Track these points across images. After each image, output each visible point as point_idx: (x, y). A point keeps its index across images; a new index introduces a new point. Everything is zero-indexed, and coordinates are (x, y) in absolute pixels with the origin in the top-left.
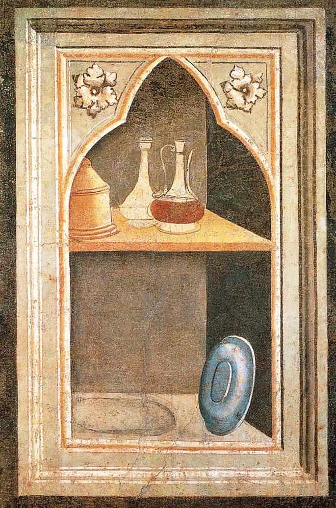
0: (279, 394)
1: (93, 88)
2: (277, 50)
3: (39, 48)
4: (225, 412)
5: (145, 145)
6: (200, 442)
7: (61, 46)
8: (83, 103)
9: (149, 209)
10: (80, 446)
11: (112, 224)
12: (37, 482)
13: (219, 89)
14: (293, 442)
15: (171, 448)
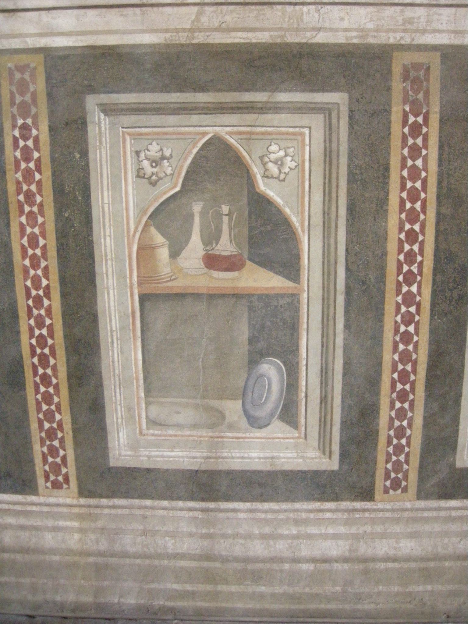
0: (304, 400)
1: (154, 161)
2: (307, 129)
3: (107, 128)
4: (261, 413)
5: (197, 208)
7: (125, 126)
8: (145, 174)
9: (201, 260)
10: (153, 435)
11: (171, 272)
12: (123, 458)
13: (258, 162)
14: (314, 432)
15: (222, 437)
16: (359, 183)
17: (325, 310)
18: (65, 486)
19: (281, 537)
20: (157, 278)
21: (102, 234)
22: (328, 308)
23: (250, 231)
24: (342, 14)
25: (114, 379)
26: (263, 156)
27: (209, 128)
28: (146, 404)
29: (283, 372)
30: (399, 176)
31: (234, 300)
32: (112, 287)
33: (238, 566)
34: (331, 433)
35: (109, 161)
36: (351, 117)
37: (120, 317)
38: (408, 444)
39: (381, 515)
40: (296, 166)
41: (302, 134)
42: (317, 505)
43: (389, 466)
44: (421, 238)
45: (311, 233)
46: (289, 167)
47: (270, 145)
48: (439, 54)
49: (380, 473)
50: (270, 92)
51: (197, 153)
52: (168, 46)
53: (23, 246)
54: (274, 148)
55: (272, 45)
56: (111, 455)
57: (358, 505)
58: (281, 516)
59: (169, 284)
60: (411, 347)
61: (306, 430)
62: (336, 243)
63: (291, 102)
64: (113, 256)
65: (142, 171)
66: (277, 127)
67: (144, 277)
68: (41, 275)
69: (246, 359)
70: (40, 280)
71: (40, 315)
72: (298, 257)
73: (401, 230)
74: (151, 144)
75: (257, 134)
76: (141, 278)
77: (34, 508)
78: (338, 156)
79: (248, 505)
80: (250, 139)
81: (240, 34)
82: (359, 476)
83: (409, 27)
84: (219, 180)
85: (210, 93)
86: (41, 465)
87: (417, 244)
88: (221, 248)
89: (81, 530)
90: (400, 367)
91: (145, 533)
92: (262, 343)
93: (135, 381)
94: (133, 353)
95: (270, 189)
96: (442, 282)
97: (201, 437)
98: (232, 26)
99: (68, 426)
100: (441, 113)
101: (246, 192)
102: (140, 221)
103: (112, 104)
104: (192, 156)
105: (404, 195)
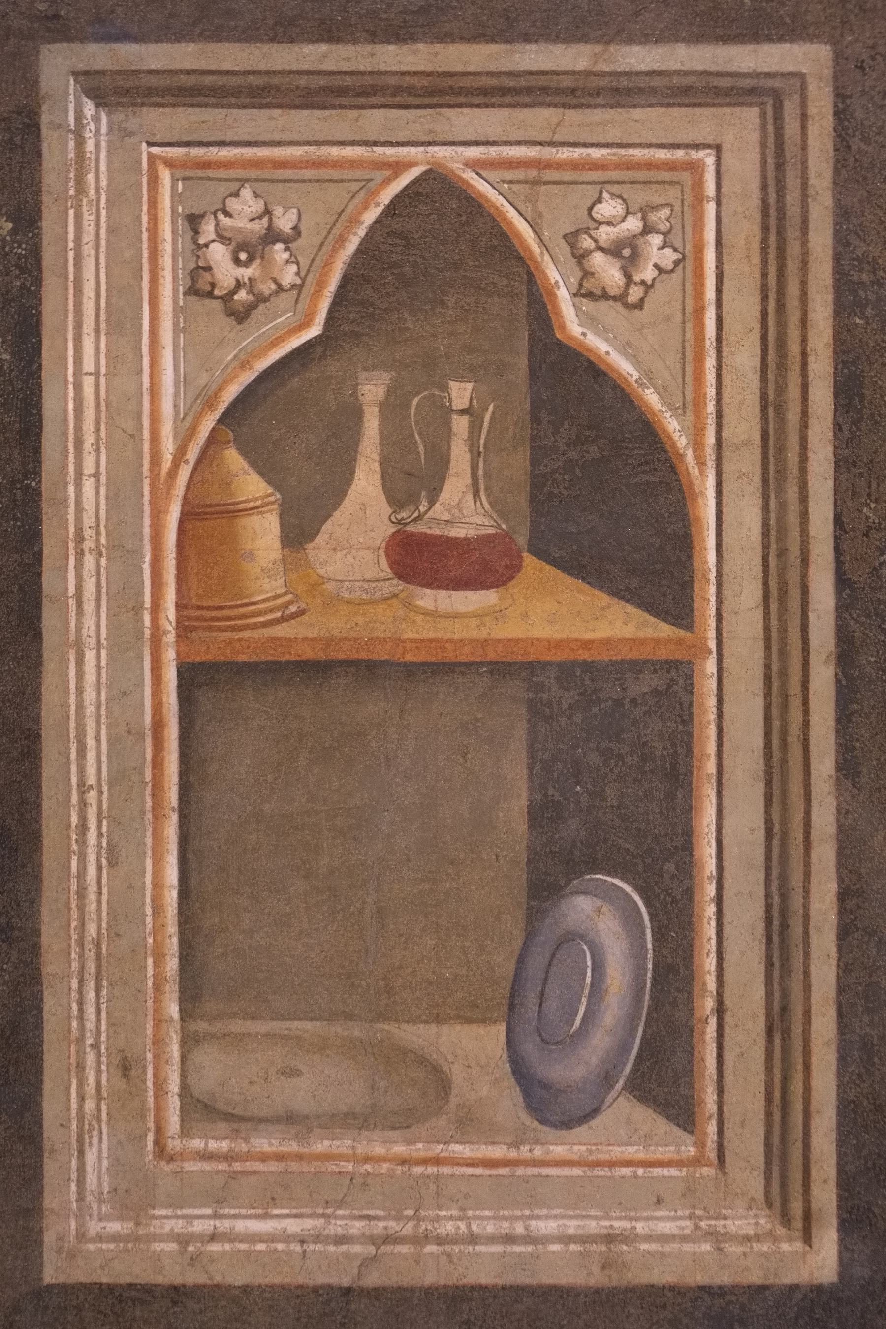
0: (713, 1022)
1: (241, 246)
2: (708, 151)
3: (103, 144)
6: (510, 1146)
7: (158, 138)
8: (213, 285)
9: (382, 552)
10: (205, 1156)
11: (286, 593)
12: (91, 1247)
15: (437, 1161)
16: (869, 312)
17: (775, 712)
20: (242, 610)
21: (71, 468)
22: (785, 707)
23: (534, 462)
25: (81, 956)
26: (576, 233)
27: (413, 150)
28: (183, 1043)
29: (641, 924)
32: (93, 641)
35: (103, 243)
36: (840, 114)
40: (677, 263)
41: (696, 168)
45: (726, 467)
46: (656, 266)
47: (599, 200)
50: (598, 41)
51: (377, 221)
54: (608, 208)
56: (49, 1238)
59: (279, 631)
61: (720, 1132)
62: (804, 499)
63: (660, 73)
64: (103, 541)
65: (207, 276)
66: (620, 145)
67: (199, 608)
74: (236, 195)
75: (559, 166)
80: (536, 182)
84: (443, 303)
85: (421, 46)
88: (446, 516)
93: (150, 961)
94: (149, 863)
95: (597, 333)
97: (367, 1159)
101: (523, 342)
103: (120, 72)
104: (362, 232)
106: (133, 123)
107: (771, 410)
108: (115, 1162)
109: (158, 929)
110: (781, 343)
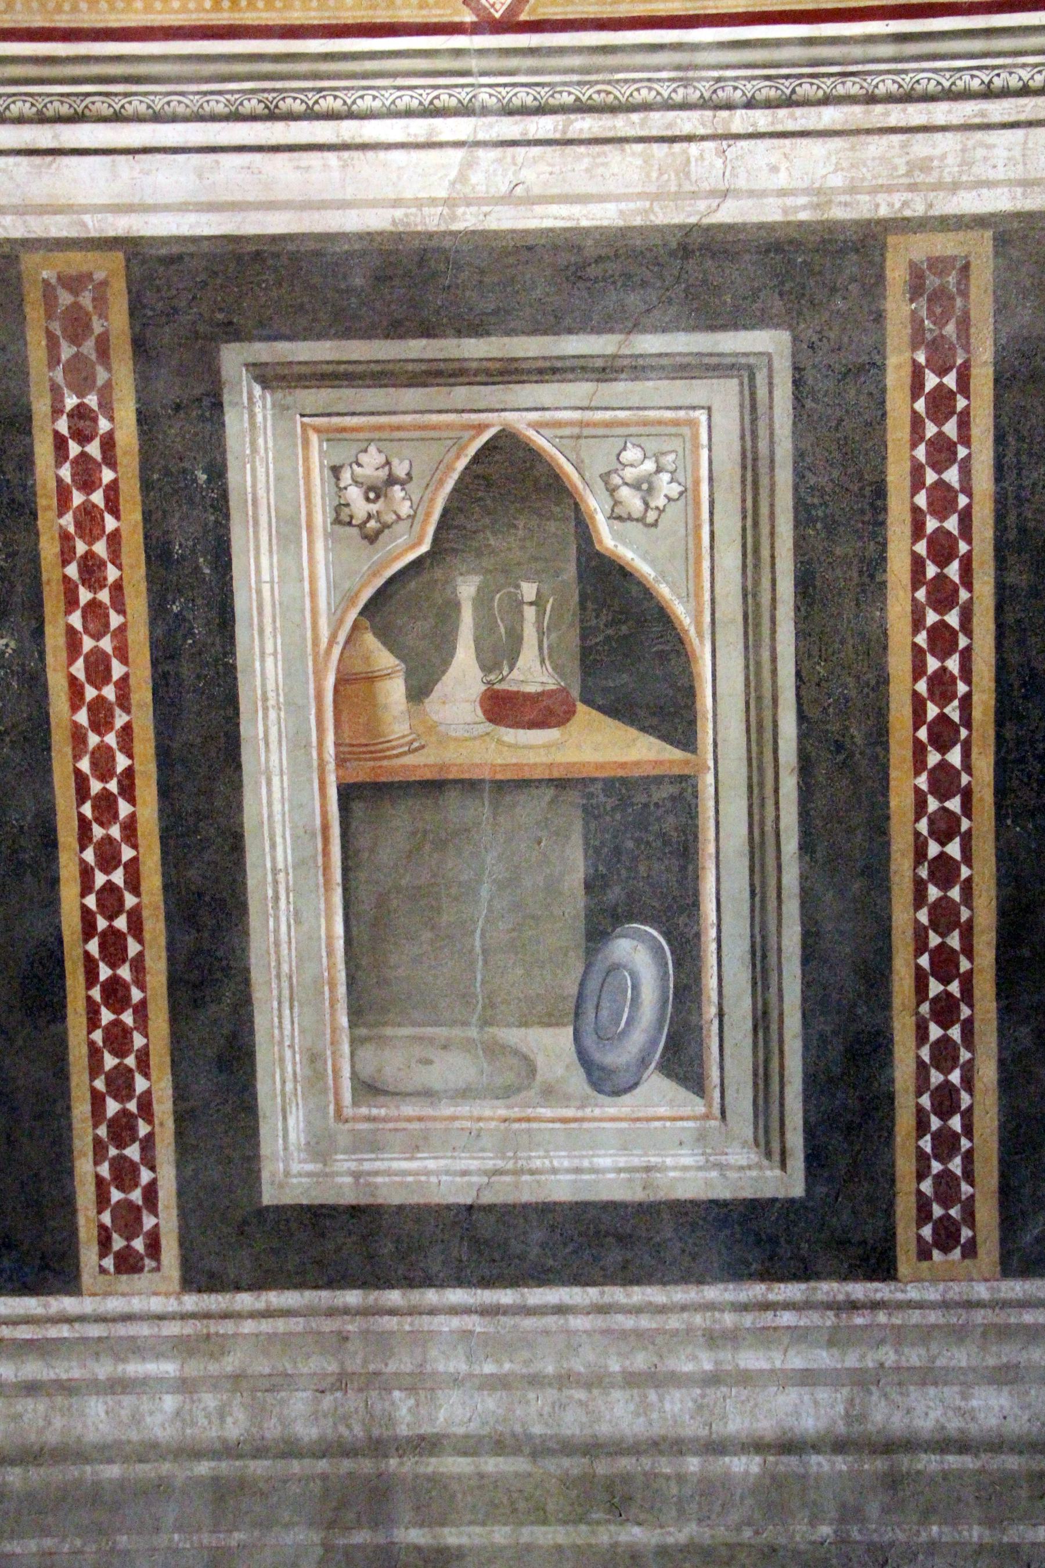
0: (716, 1023)
1: (371, 488)
3: (269, 417)
6: (578, 1108)
7: (308, 411)
8: (351, 517)
9: (477, 704)
12: (295, 1181)
14: (742, 1101)
15: (528, 1120)
16: (819, 526)
17: (756, 810)
18: (149, 1263)
19: (675, 1380)
20: (380, 747)
21: (257, 650)
22: (762, 806)
23: (583, 638)
24: (774, 158)
25: (279, 986)
26: (609, 473)
27: (490, 415)
28: (352, 1042)
29: (664, 957)
30: (907, 507)
31: (551, 792)
32: (277, 770)
33: (574, 1465)
34: (782, 1105)
35: (272, 487)
36: (797, 383)
37: (295, 838)
38: (968, 1130)
39: (915, 1317)
40: (681, 494)
41: (693, 424)
42: (757, 1290)
43: (927, 1186)
44: (963, 642)
46: (666, 496)
47: (624, 449)
48: (989, 234)
49: (905, 1207)
50: (621, 332)
51: (466, 468)
52: (398, 237)
53: (73, 680)
54: (631, 454)
55: (623, 232)
56: (265, 1175)
57: (858, 1290)
58: (674, 1322)
59: (408, 760)
60: (955, 893)
61: (722, 1097)
62: (774, 659)
63: (667, 355)
64: (281, 700)
65: (346, 510)
66: (638, 408)
68: (114, 745)
69: (581, 924)
70: (113, 758)
71: (108, 839)
72: (690, 693)
73: (917, 624)
74: (366, 451)
75: (595, 425)
76: (341, 749)
77: (64, 1331)
78: (772, 469)
79: (592, 1294)
80: (579, 437)
81: (554, 209)
82: (854, 1212)
83: (920, 178)
84: (515, 527)
85: (493, 339)
86: (92, 1212)
87: (956, 657)
88: (522, 678)
89: (185, 1386)
90: (934, 940)
91: (342, 1381)
92: (617, 889)
93: (326, 988)
94: (323, 921)
95: (624, 544)
96: (1019, 742)
97: (479, 1119)
98: (536, 191)
99: (164, 1108)
100: (995, 364)
102: (341, 622)
103: (278, 364)
104: (455, 476)
105: (921, 548)
106: (289, 400)
107: (750, 596)
108: (308, 1123)
109: (331, 967)
110: (756, 551)
